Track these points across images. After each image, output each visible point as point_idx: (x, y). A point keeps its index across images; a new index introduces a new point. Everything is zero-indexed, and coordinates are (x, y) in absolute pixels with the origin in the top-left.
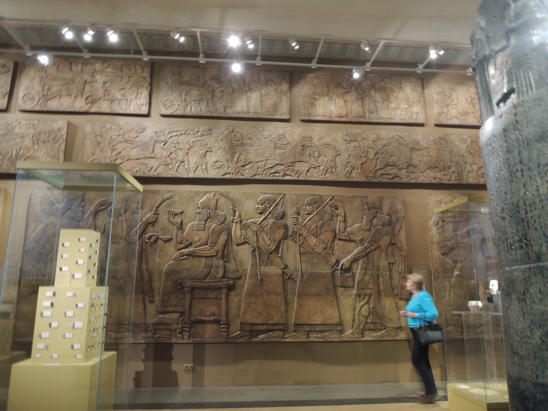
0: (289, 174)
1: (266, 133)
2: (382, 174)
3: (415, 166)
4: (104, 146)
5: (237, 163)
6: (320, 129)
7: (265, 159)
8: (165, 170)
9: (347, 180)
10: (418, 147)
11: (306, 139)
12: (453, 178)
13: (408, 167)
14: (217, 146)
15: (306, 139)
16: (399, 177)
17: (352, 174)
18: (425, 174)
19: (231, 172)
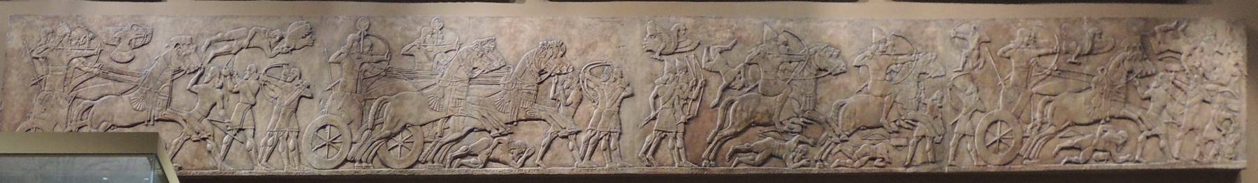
0: (502, 158)
1: (449, 36)
2: (736, 151)
3: (824, 124)
4: (52, 90)
5: (374, 126)
6: (587, 21)
7: (444, 115)
8: (196, 156)
9: (646, 170)
10: (839, 64)
11: (550, 52)
12: (919, 159)
13: (804, 126)
14: (326, 82)
15: (550, 52)
16: (780, 158)
17: (660, 153)
18: (848, 148)
19: (357, 158)
